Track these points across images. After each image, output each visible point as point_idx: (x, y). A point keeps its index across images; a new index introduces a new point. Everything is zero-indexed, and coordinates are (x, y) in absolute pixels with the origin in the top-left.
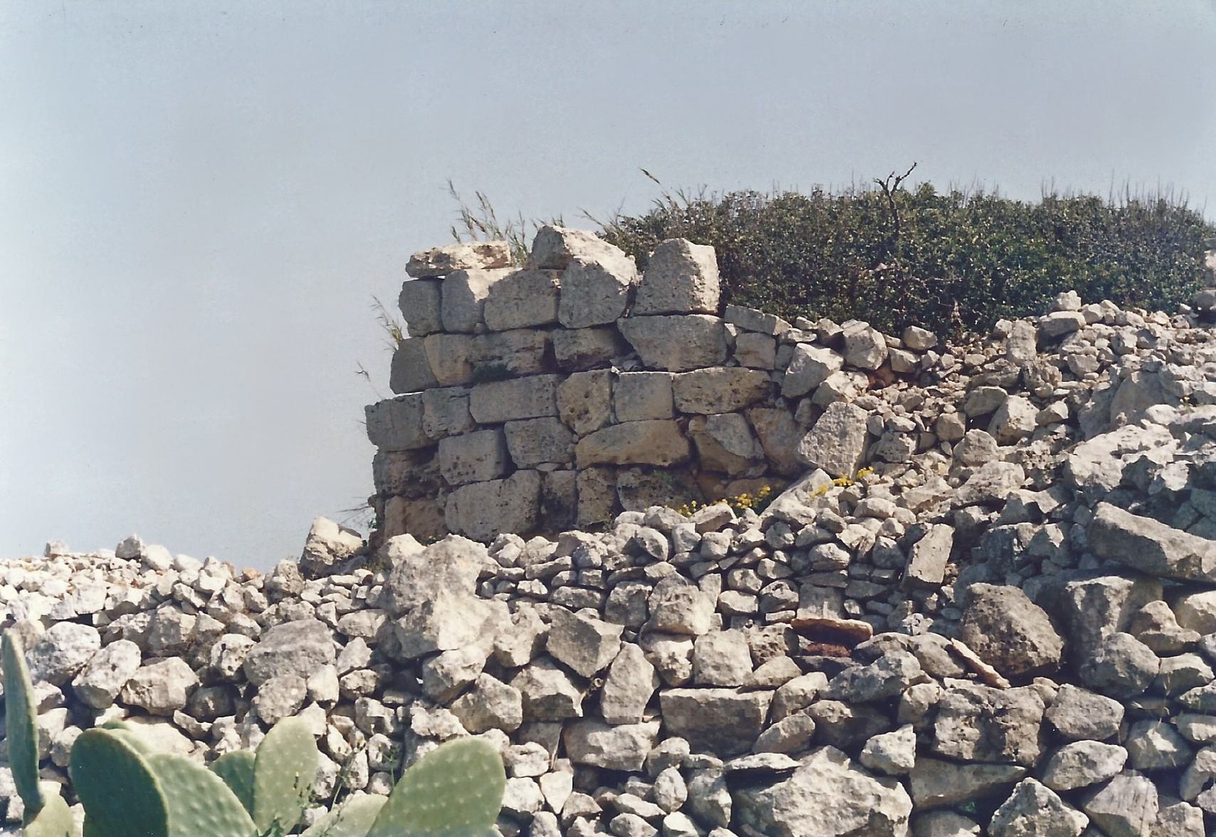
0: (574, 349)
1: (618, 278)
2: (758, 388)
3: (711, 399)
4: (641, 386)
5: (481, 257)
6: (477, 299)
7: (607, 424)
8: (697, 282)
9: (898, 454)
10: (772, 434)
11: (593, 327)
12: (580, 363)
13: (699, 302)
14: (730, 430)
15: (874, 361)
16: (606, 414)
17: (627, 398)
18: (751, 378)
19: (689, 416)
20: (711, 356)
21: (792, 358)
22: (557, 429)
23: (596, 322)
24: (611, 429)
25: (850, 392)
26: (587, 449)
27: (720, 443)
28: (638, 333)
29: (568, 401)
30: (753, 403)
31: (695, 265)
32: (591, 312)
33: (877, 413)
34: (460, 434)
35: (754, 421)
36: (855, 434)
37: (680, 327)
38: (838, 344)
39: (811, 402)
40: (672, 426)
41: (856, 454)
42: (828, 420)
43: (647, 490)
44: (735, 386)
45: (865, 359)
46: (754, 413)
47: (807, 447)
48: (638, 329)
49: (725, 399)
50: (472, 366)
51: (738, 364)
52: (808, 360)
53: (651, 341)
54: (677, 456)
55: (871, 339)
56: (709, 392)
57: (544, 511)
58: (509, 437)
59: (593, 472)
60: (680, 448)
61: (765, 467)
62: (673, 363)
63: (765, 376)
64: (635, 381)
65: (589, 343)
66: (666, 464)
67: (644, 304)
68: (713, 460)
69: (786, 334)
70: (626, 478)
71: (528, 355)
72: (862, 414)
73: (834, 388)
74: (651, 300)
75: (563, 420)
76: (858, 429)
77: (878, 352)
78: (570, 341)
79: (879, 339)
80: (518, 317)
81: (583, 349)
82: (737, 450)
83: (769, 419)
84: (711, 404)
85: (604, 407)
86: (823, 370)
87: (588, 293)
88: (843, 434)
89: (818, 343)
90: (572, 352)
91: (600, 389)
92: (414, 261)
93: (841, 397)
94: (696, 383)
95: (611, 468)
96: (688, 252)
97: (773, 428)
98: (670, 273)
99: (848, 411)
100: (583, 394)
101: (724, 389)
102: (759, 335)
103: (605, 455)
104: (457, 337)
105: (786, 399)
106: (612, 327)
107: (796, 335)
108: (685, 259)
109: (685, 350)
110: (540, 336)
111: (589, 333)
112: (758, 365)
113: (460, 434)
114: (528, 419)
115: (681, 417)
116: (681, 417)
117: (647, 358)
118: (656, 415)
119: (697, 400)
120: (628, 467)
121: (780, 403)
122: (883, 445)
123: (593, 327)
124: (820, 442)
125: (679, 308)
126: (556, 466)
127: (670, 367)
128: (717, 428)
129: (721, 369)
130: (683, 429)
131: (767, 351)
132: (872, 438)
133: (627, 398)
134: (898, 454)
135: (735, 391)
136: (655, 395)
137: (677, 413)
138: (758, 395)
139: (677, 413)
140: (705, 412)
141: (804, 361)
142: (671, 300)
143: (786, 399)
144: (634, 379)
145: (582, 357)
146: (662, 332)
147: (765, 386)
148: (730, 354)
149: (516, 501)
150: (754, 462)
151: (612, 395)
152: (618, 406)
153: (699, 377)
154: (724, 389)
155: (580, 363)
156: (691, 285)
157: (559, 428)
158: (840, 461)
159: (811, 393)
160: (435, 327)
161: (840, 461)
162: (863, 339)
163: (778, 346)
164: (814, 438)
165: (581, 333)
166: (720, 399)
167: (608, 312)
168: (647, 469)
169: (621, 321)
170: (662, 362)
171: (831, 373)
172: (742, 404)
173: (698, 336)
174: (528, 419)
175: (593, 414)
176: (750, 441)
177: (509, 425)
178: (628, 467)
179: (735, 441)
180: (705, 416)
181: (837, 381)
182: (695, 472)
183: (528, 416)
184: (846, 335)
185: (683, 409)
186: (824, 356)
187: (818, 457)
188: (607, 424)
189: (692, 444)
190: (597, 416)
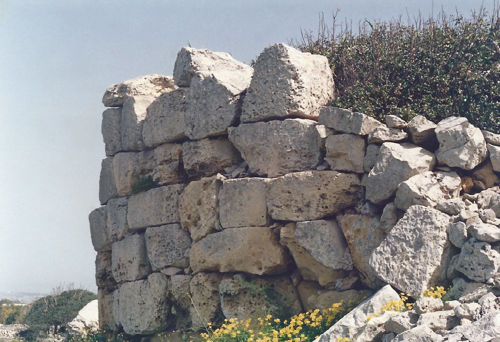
0: (196, 159)
1: (229, 88)
2: (348, 193)
3: (300, 205)
4: (240, 193)
5: (160, 88)
6: (140, 119)
7: (213, 230)
8: (294, 85)
9: (480, 271)
10: (360, 243)
11: (211, 138)
12: (202, 171)
13: (295, 105)
14: (318, 238)
15: (466, 158)
16: (212, 220)
17: (229, 205)
18: (338, 181)
19: (284, 223)
20: (305, 160)
21: (378, 156)
22: (176, 233)
23: (211, 132)
24: (215, 235)
25: (434, 194)
26: (198, 255)
27: (309, 252)
28: (243, 138)
29: (186, 208)
30: (343, 210)
31: (292, 68)
32: (207, 123)
33: (460, 219)
34: (123, 238)
35: (343, 227)
36: (431, 244)
37: (280, 134)
38: (429, 143)
39: (389, 203)
40: (265, 234)
41: (431, 269)
42: (403, 228)
43: (247, 298)
44: (323, 191)
45: (457, 156)
46: (343, 219)
47: (378, 261)
48: (243, 137)
49: (314, 206)
50: (137, 176)
51: (329, 168)
52: (392, 160)
53: (253, 148)
54: (271, 265)
55: (465, 134)
56: (298, 198)
57: (174, 311)
58: (148, 241)
59: (202, 278)
60: (273, 257)
61: (355, 279)
62: (272, 169)
63: (354, 179)
64: (235, 187)
65: (207, 152)
66: (260, 273)
67: (249, 111)
68: (307, 269)
69: (372, 133)
70: (227, 285)
71: (166, 167)
72: (443, 220)
73: (415, 189)
74: (254, 107)
75: (183, 227)
76: (435, 238)
77: (473, 149)
78: (193, 151)
79: (476, 135)
80: (161, 134)
81: (202, 159)
82: (325, 260)
83: (358, 227)
84: (300, 210)
85: (211, 214)
86: (405, 170)
87: (205, 105)
88: (419, 244)
89: (409, 141)
90: (194, 162)
91: (209, 197)
92: (108, 93)
93: (423, 200)
94: (286, 188)
95: (214, 272)
96: (287, 56)
97: (361, 236)
98: (270, 79)
99: (426, 217)
100: (196, 201)
101: (311, 194)
102: (347, 136)
103: (211, 261)
104: (128, 154)
105: (371, 204)
106: (223, 137)
107: (382, 132)
108: (283, 63)
109: (283, 155)
110: (175, 149)
111: (206, 143)
112: (348, 168)
113: (123, 238)
114: (159, 226)
115: (274, 223)
116: (274, 223)
117: (252, 165)
118: (252, 222)
119: (287, 206)
120: (231, 274)
121: (365, 209)
122: (464, 258)
123: (211, 138)
124: (393, 253)
125: (277, 113)
126: (179, 270)
127: (270, 173)
128: (305, 235)
129: (310, 173)
130: (276, 237)
131: (355, 152)
132: (452, 250)
133: (229, 205)
134: (480, 271)
135: (323, 196)
136: (249, 203)
137: (271, 220)
138: (347, 200)
139: (271, 220)
140: (294, 219)
141: (388, 161)
142: (271, 105)
143: (371, 204)
144: (235, 186)
145: (203, 166)
146: (262, 139)
147: (353, 190)
148: (320, 157)
149: (150, 302)
150: (344, 273)
151: (218, 202)
152: (222, 212)
153: (288, 182)
154: (311, 194)
155: (202, 171)
156: (287, 87)
157: (180, 234)
158: (411, 277)
159: (392, 199)
160: (118, 148)
161: (411, 277)
162: (455, 134)
163: (367, 145)
164: (387, 248)
165: (200, 144)
166: (308, 205)
167: (221, 122)
168: (248, 277)
169: (230, 129)
170: (263, 169)
171: (415, 172)
172: (331, 210)
173: (294, 141)
174: (159, 226)
175: (203, 222)
176: (341, 250)
177: (148, 231)
178: (231, 274)
179: (322, 250)
180: (295, 223)
181: (421, 182)
182: (295, 280)
183: (159, 223)
184: (437, 131)
185: (274, 216)
186: (415, 157)
187: (388, 271)
188: (213, 230)
189: (287, 254)
190: (206, 223)
